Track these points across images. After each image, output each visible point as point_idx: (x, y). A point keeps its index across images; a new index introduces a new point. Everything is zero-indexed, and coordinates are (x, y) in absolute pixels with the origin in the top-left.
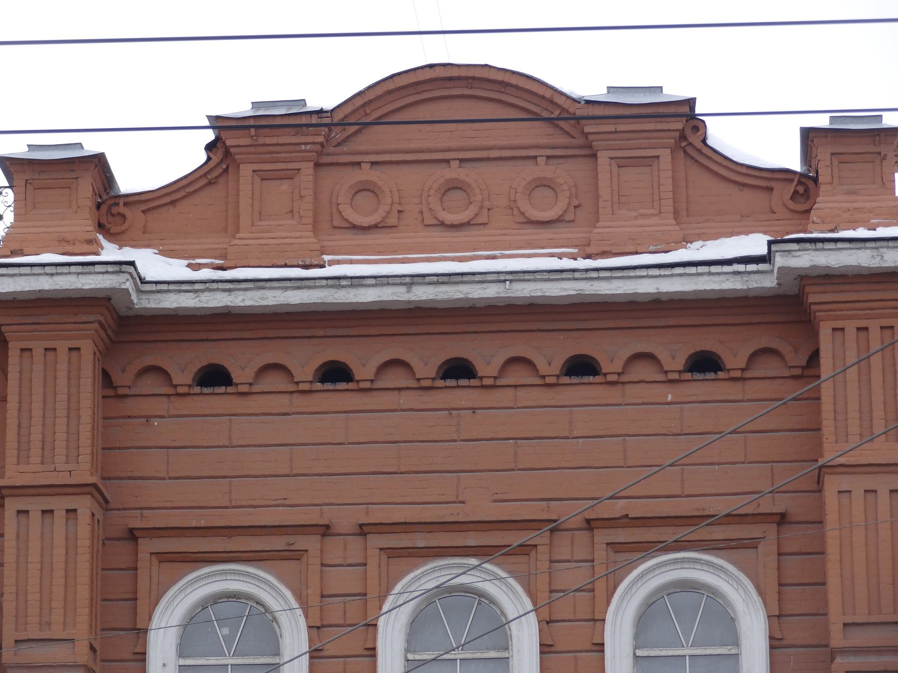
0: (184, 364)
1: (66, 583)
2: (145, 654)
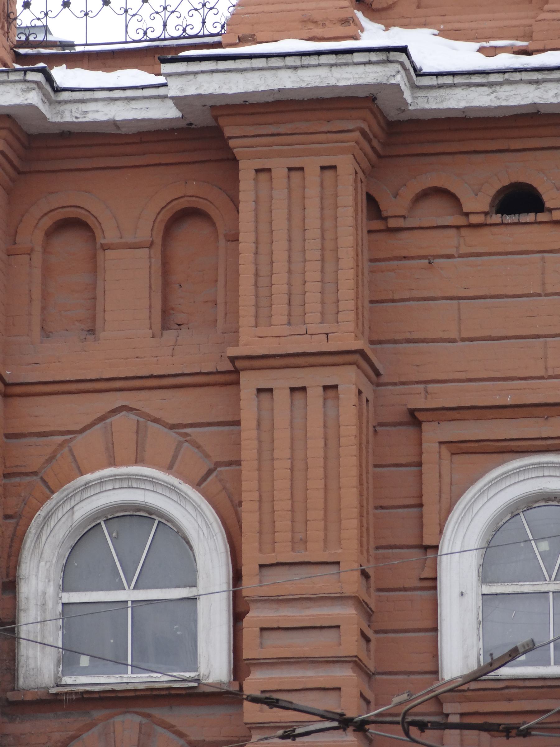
0: (478, 182)
1: (326, 486)
2: (435, 579)
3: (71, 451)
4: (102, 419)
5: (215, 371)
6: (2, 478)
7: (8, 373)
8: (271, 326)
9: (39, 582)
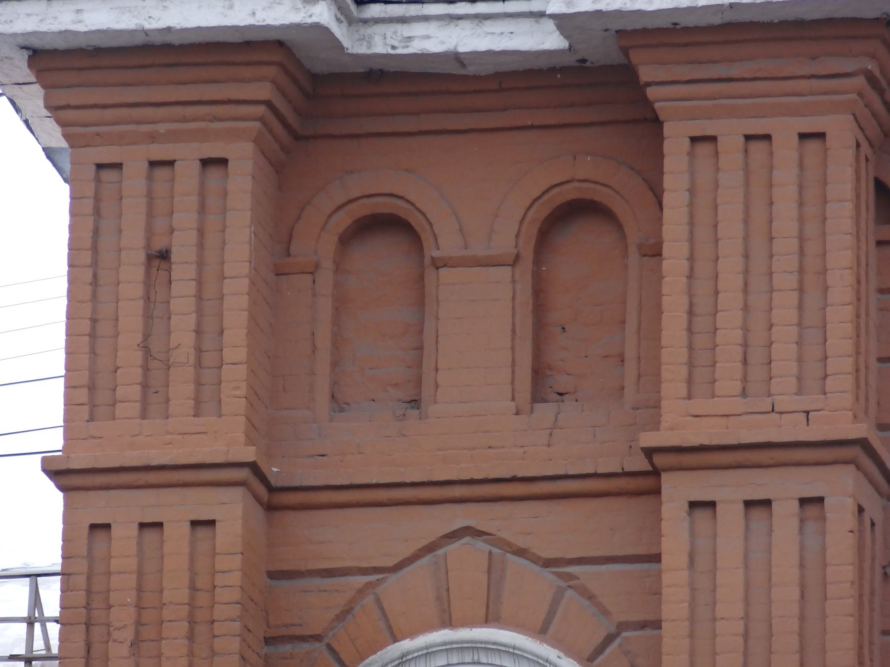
3: (378, 601)
4: (430, 548)
5: (620, 471)
6: (263, 644)
7: (275, 470)
8: (713, 396)
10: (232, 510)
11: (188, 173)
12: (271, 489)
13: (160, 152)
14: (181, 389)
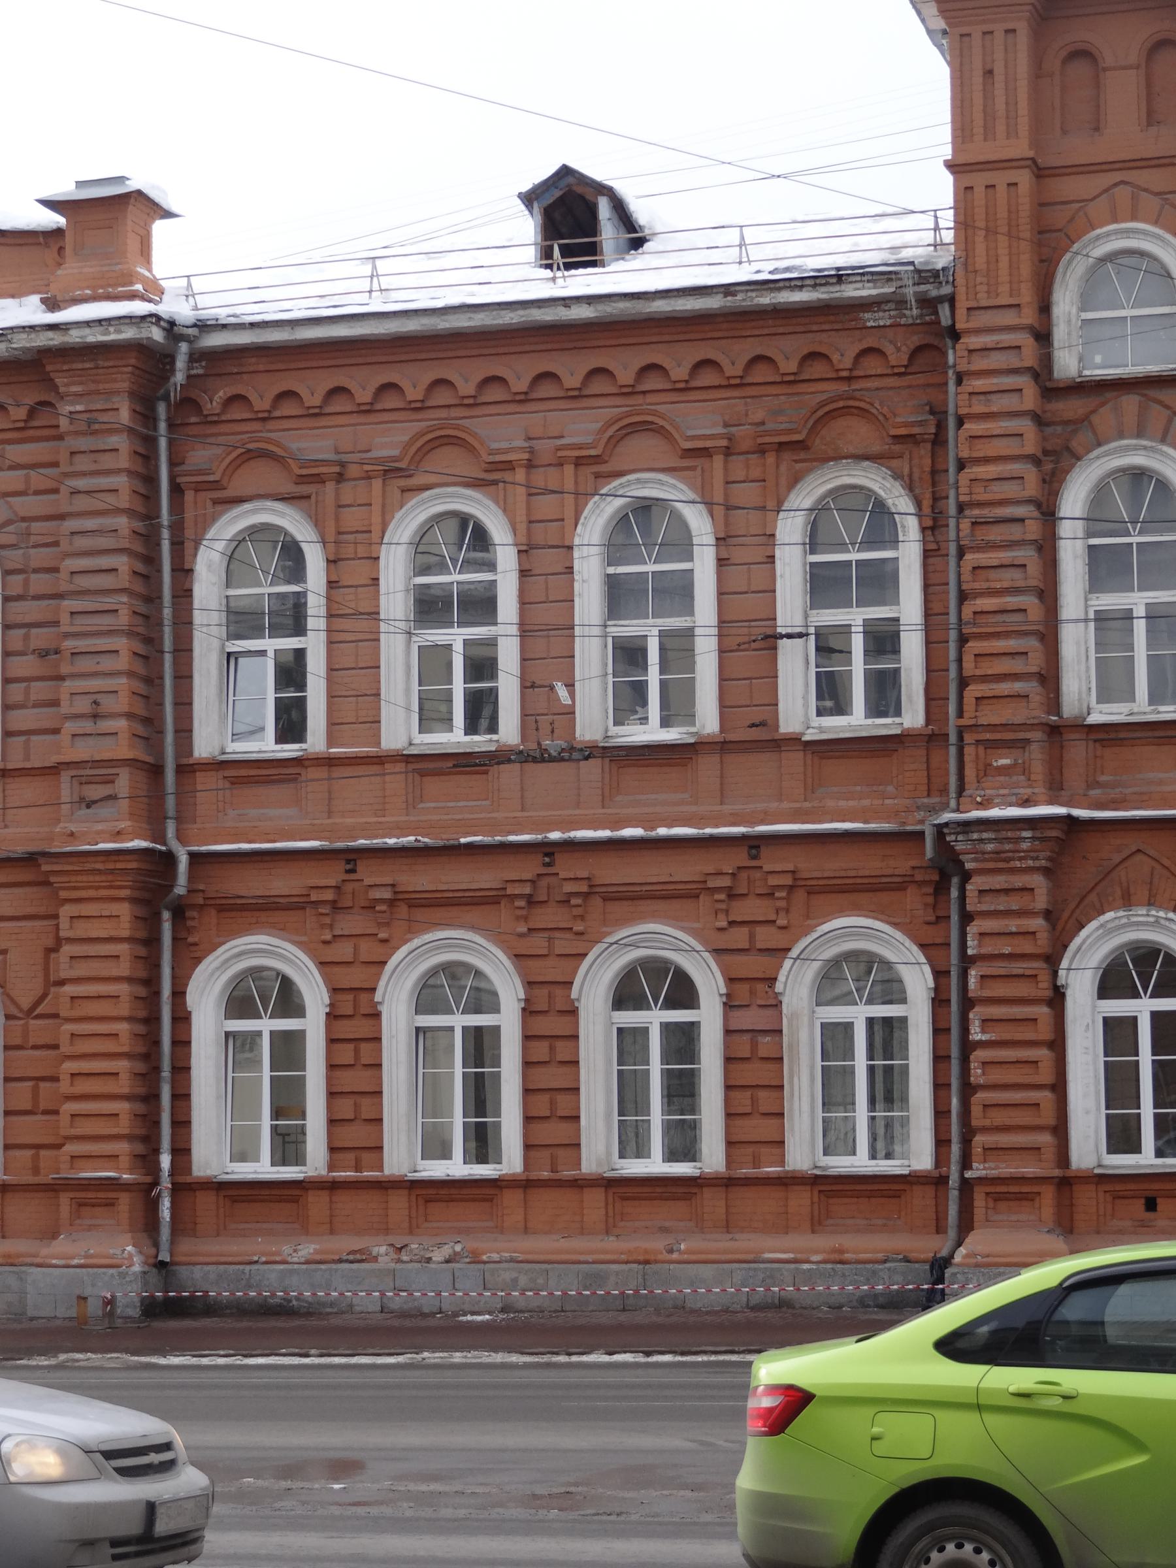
3: (1086, 214)
4: (1106, 191)
9: (1065, 303)
10: (1024, 178)
11: (999, 36)
12: (1039, 169)
13: (987, 28)
14: (1001, 128)
